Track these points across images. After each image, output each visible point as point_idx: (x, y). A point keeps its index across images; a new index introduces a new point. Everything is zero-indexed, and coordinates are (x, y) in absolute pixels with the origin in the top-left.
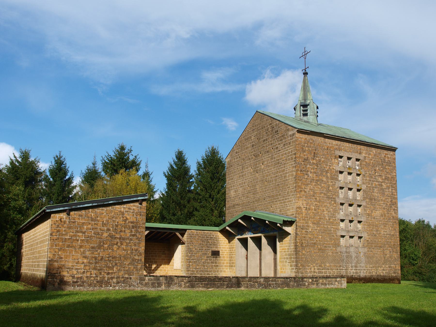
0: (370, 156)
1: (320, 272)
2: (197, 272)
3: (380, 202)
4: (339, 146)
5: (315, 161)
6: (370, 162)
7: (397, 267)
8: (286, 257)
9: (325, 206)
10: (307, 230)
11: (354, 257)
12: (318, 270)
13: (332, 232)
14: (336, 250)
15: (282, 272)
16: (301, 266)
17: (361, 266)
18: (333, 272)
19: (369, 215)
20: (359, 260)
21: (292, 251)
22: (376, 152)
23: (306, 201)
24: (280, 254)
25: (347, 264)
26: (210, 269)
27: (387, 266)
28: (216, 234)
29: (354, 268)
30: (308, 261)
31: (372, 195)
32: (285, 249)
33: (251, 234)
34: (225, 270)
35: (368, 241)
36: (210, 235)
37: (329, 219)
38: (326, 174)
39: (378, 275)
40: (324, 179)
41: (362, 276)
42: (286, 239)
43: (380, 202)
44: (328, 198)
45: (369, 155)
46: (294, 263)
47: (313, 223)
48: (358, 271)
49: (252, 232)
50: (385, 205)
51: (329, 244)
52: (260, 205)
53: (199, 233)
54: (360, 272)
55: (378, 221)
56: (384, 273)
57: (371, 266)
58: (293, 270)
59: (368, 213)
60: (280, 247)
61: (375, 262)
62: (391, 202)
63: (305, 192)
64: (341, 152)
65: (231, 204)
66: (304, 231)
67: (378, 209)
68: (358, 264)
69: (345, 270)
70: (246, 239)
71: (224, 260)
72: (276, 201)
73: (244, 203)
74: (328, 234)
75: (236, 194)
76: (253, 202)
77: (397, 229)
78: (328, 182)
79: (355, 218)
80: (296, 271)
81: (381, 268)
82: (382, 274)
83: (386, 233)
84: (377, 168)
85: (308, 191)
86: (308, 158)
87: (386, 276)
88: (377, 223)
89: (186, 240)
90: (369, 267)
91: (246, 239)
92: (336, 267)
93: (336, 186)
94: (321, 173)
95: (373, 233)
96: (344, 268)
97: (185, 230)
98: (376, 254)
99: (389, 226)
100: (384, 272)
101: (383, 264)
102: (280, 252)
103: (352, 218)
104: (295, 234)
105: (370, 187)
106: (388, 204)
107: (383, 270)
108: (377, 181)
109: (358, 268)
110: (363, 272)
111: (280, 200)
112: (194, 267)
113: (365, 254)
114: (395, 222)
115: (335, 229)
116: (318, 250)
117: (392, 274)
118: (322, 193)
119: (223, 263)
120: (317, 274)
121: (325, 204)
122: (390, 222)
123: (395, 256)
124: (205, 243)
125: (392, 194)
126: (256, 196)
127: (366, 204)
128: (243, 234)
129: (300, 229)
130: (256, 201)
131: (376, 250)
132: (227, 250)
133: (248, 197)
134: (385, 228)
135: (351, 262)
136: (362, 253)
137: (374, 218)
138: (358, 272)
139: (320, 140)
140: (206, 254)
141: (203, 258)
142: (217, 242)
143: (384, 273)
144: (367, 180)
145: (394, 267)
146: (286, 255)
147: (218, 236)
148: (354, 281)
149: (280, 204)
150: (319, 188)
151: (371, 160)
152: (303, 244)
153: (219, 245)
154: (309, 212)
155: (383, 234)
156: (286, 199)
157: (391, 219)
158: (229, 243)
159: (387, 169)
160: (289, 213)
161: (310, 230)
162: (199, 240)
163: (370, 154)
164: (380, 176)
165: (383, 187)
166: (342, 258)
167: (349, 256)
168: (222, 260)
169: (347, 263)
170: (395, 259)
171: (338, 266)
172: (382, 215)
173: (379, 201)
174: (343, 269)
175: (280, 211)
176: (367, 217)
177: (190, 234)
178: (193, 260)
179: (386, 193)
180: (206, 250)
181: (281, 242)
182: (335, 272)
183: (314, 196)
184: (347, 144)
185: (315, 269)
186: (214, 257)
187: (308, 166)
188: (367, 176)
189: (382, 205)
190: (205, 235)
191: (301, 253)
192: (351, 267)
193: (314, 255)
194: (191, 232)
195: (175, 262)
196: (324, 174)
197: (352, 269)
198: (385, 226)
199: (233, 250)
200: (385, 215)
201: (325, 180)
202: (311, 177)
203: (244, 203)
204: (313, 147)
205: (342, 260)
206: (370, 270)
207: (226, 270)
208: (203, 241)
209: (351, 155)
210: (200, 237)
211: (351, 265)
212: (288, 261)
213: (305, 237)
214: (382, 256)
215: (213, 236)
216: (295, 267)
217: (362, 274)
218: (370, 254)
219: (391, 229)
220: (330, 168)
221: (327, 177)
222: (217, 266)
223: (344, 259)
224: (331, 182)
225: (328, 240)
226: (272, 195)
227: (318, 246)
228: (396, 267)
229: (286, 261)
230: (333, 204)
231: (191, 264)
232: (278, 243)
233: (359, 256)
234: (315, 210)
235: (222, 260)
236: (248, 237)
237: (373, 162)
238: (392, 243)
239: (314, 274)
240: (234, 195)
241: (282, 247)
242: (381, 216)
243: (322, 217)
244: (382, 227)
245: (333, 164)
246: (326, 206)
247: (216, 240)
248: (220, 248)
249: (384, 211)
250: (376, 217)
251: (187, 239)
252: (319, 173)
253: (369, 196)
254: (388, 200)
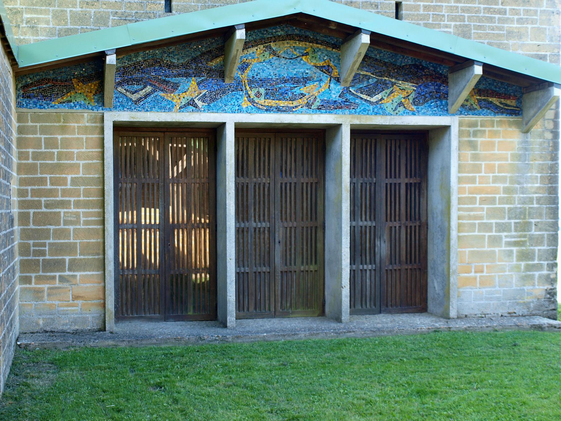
8: (493, 221)
21: (531, 200)
24: (459, 209)
32: (496, 191)
46: (541, 243)
58: (537, 274)
146: (493, 213)
212: (504, 240)
216: (547, 259)
229: (495, 241)
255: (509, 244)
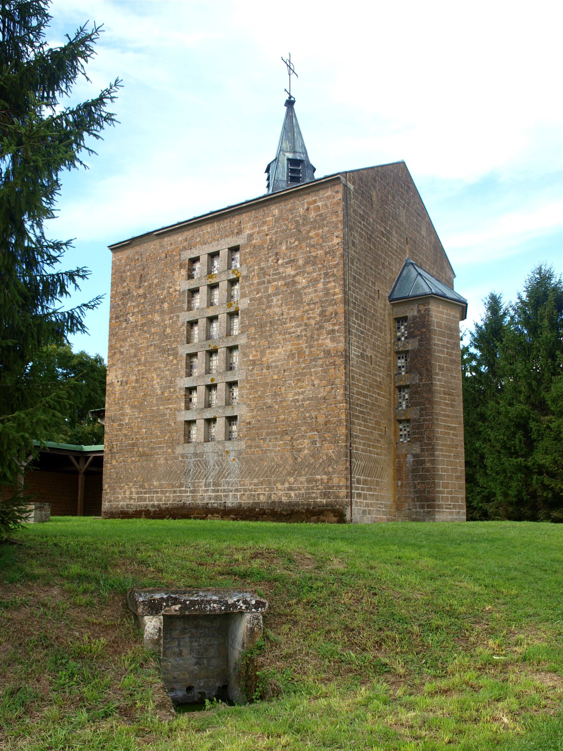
0: (265, 228)
1: (140, 499)
3: (288, 325)
4: (189, 240)
5: (141, 291)
6: (264, 241)
7: (335, 480)
9: (155, 369)
10: (122, 423)
11: (212, 463)
12: (137, 494)
13: (167, 417)
14: (174, 453)
16: (108, 487)
17: (228, 483)
18: (165, 497)
19: (254, 363)
20: (224, 469)
22: (281, 211)
23: (121, 369)
25: (195, 480)
27: (303, 479)
29: (212, 488)
30: (121, 478)
31: (265, 314)
35: (249, 423)
37: (163, 393)
38: (160, 306)
39: (274, 502)
40: (157, 318)
41: (230, 505)
43: (288, 325)
44: (163, 351)
45: (262, 226)
47: (133, 407)
48: (222, 494)
50: (304, 327)
51: (160, 443)
54: (226, 496)
55: (279, 372)
56: (290, 497)
57: (255, 481)
59: (252, 360)
61: (266, 471)
62: (320, 315)
63: (121, 353)
64: (193, 250)
66: (116, 425)
67: (282, 342)
68: (222, 478)
69: (191, 492)
74: (159, 422)
77: (337, 381)
78: (163, 320)
79: (219, 377)
81: (283, 484)
82: (284, 499)
83: (301, 397)
84: (284, 248)
85: (127, 350)
86: (129, 290)
87: (297, 504)
88: (275, 377)
90: (251, 484)
92: (173, 487)
93: (180, 324)
94: (150, 309)
95: (265, 404)
96: (189, 488)
98: (271, 451)
99: (313, 378)
100: (292, 494)
101: (290, 474)
103: (212, 380)
105: (261, 298)
106: (313, 322)
107: (290, 489)
108: (279, 279)
109: (222, 488)
110: (235, 496)
113: (240, 454)
114: (334, 364)
115: (173, 409)
116: (139, 456)
117: (317, 498)
118: (151, 345)
120: (135, 501)
121: (156, 365)
122: (316, 366)
123: (331, 451)
125: (327, 294)
127: (249, 339)
129: (110, 421)
131: (270, 441)
134: (300, 384)
135: (205, 476)
136: (232, 454)
137: (268, 368)
138: (221, 496)
139: (152, 246)
143: (293, 495)
144: (253, 284)
145: (325, 481)
148: (210, 515)
150: (146, 338)
151: (267, 235)
152: (113, 447)
154: (126, 387)
155: (291, 401)
157: (320, 358)
159: (312, 238)
161: (127, 421)
163: (264, 223)
164: (293, 261)
165: (300, 287)
166: (184, 468)
167: (200, 463)
169: (197, 477)
170: (330, 459)
171: (177, 485)
172: (291, 356)
173: (285, 323)
174: (186, 492)
176: (248, 369)
179: (306, 299)
182: (169, 497)
183: (135, 356)
184: (208, 228)
185: (131, 493)
187: (129, 305)
188: (254, 276)
189: (294, 329)
191: (109, 465)
192: (206, 485)
193: (132, 467)
196: (158, 307)
197: (207, 490)
198: (298, 380)
200: (301, 353)
201: (159, 318)
202: (132, 322)
204: (138, 266)
205: (185, 473)
206: (251, 491)
209: (218, 245)
211: (204, 481)
213: (116, 436)
214: (288, 454)
217: (231, 502)
218: (253, 453)
219: (319, 384)
220: (168, 292)
221: (162, 312)
223: (190, 470)
224: (170, 318)
225: (159, 434)
227: (138, 448)
228: (330, 479)
230: (172, 361)
233: (224, 461)
234: (137, 381)
237: (271, 239)
238: (321, 420)
239: (129, 501)
242: (288, 357)
243: (149, 392)
244: (289, 384)
245: (177, 282)
246: (159, 368)
249: (299, 344)
250: (273, 364)
252: (148, 309)
253: (256, 320)
254: (313, 313)
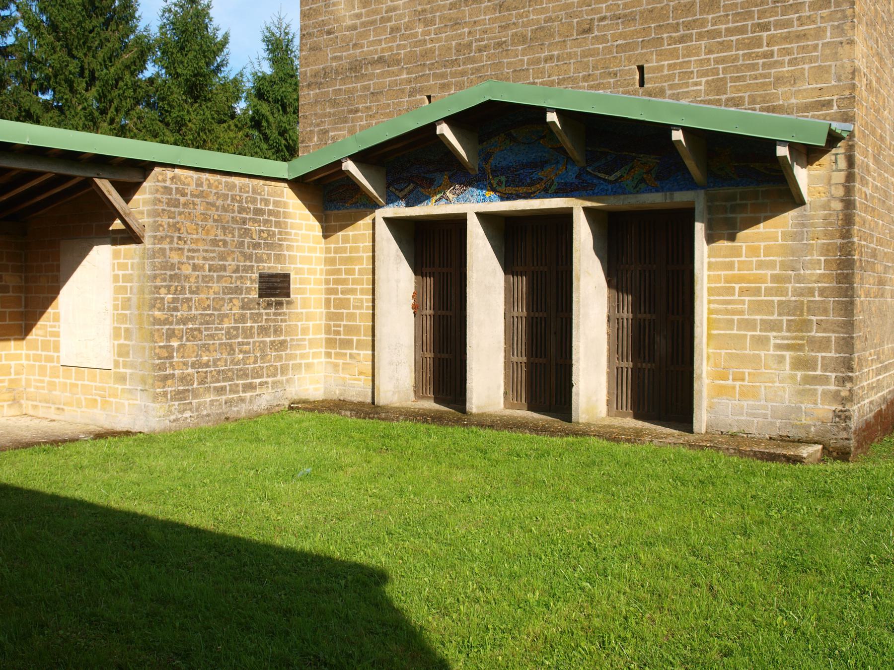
2: (202, 382)
8: (758, 317)
15: (720, 391)
21: (811, 292)
24: (710, 302)
26: (255, 362)
28: (274, 194)
32: (761, 279)
33: (484, 200)
34: (310, 360)
36: (254, 201)
42: (761, 228)
46: (827, 349)
49: (494, 190)
52: (550, 58)
53: (210, 185)
58: (820, 389)
60: (711, 266)
65: (334, 58)
70: (459, 223)
71: (309, 317)
72: (682, 39)
73: (432, 50)
75: (375, 12)
76: (500, 44)
80: (843, 394)
89: (145, 220)
91: (459, 223)
97: (144, 168)
102: (711, 291)
104: (838, 206)
111: (712, 34)
112: (190, 360)
119: (305, 331)
124: (234, 236)
126: (521, 16)
128: (428, 198)
130: (523, 39)
132: (318, 268)
133: (457, 24)
140: (237, 290)
141: (225, 309)
142: (280, 233)
146: (757, 307)
147: (285, 205)
149: (710, 52)
153: (289, 248)
156: (765, 27)
158: (325, 237)
160: (783, 95)
162: (210, 223)
168: (299, 316)
175: (718, 87)
177: (167, 190)
178: (184, 321)
180: (237, 270)
181: (723, 244)
186: (269, 305)
190: (233, 199)
194: (172, 178)
195: (63, 328)
199: (349, 272)
203: (425, 54)
207: (315, 361)
208: (224, 228)
210: (213, 205)
212: (772, 341)
215: (266, 202)
216: (835, 370)
222: (283, 343)
226: (651, 11)
229: (761, 342)
231: (175, 343)
232: (702, 249)
235: (299, 316)
236: (465, 214)
240: (358, 16)
241: (730, 266)
247: (278, 224)
248: (292, 259)
251: (155, 214)
255: (779, 347)
